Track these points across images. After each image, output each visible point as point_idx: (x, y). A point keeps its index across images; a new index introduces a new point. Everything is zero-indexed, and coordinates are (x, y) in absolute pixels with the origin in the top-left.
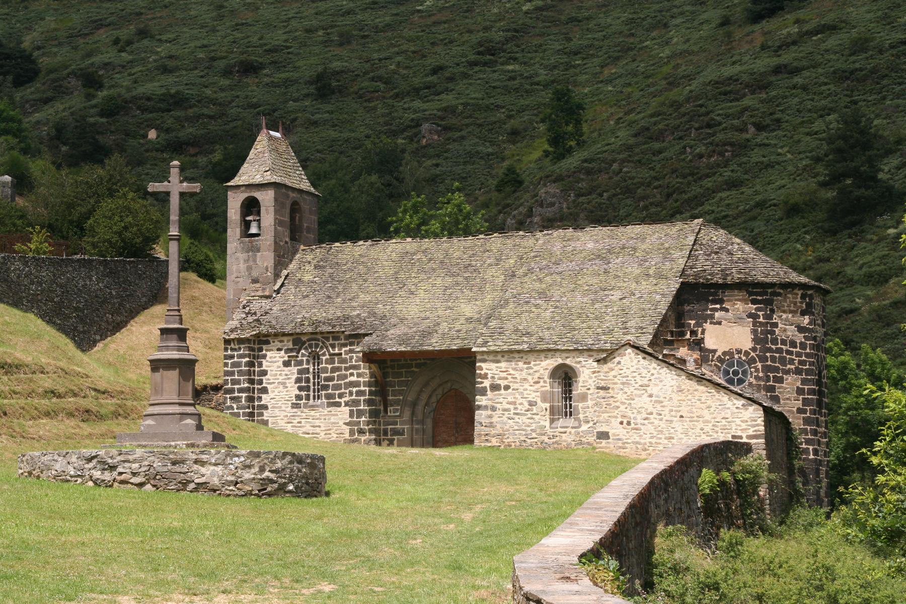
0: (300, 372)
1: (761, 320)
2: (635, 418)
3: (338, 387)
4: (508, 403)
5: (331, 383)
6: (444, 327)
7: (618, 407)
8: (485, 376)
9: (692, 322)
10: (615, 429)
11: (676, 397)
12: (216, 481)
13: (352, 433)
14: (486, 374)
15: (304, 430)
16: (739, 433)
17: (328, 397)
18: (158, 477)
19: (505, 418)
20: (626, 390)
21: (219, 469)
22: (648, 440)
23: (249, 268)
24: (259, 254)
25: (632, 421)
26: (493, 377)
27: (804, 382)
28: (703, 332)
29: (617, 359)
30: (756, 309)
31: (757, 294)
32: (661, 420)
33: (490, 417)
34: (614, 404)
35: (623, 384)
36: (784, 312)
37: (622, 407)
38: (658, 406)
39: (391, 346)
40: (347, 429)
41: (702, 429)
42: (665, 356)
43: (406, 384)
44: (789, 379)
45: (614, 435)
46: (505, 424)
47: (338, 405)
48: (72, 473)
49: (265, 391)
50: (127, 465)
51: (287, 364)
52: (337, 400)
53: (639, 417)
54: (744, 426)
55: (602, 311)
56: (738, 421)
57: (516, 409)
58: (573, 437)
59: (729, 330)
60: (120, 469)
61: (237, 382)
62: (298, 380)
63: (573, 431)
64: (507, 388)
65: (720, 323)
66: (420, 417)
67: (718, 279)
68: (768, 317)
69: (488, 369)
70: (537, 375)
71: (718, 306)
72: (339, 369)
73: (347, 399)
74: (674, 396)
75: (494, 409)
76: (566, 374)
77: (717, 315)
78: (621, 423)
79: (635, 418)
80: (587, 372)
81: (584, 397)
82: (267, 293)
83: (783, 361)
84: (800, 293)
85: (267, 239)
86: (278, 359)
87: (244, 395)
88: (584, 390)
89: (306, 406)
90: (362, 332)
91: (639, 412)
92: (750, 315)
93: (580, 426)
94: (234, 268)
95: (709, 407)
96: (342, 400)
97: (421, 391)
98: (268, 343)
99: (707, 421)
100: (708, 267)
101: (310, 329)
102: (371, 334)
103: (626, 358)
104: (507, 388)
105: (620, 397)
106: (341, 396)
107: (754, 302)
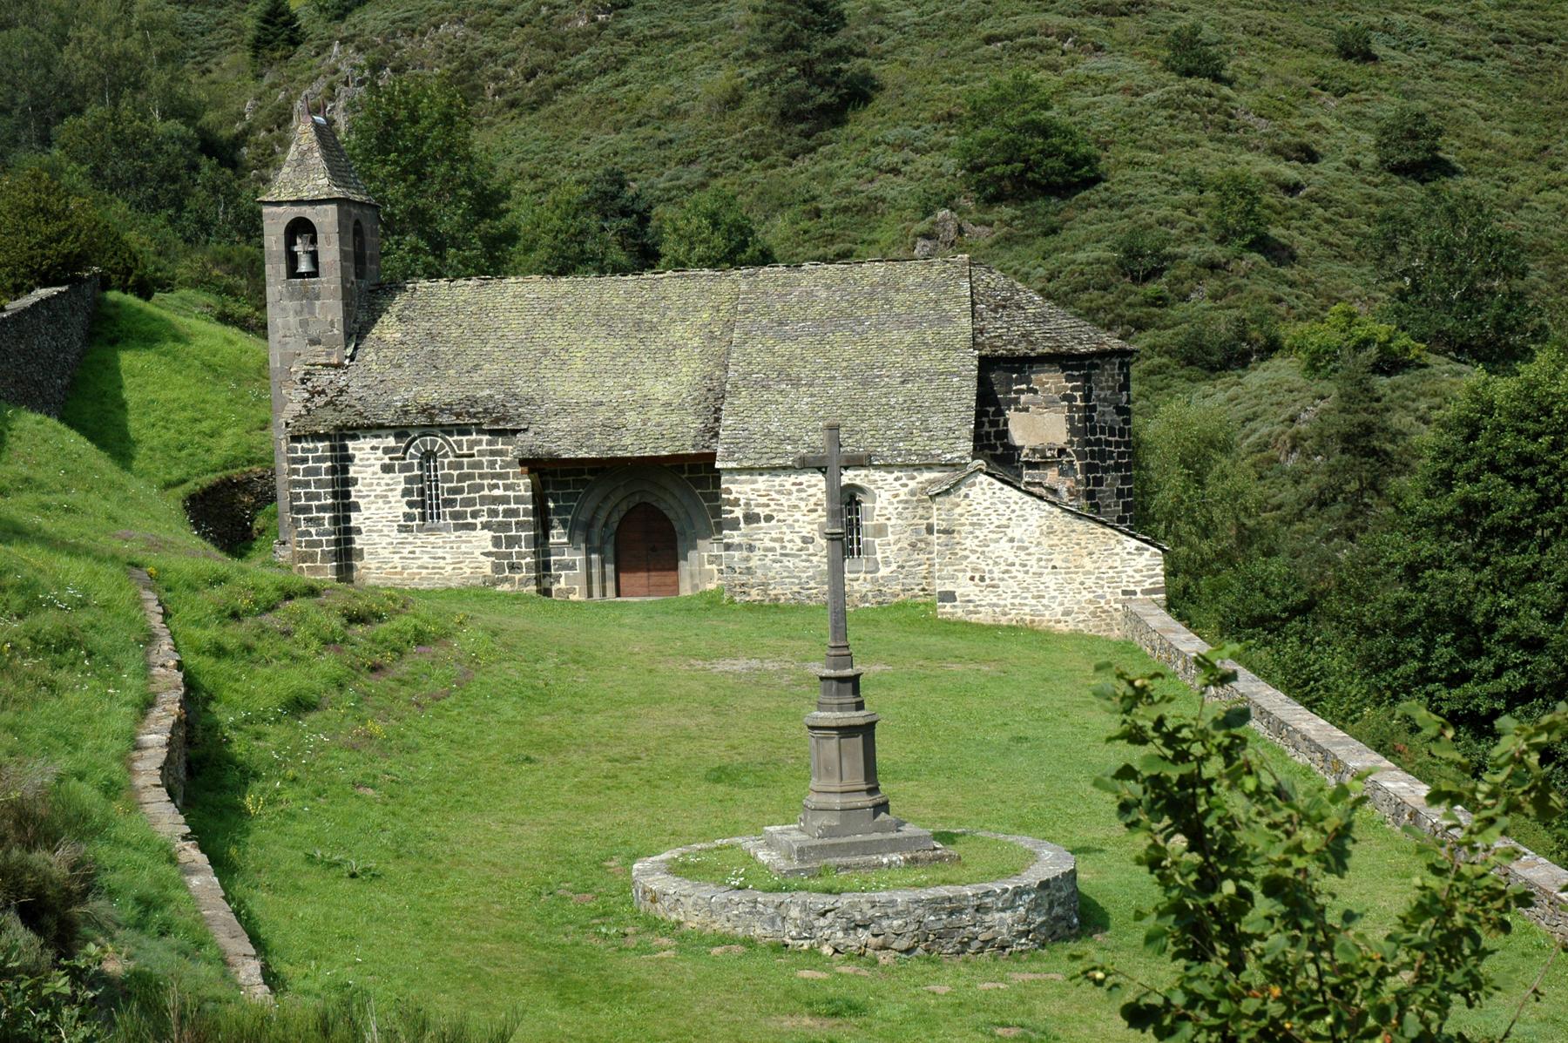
0: (408, 480)
1: (1078, 403)
2: (991, 572)
3: (469, 502)
4: (773, 540)
5: (458, 497)
6: (631, 417)
7: (966, 557)
8: (736, 503)
9: (992, 409)
10: (964, 588)
11: (1045, 541)
12: (1004, 935)
13: (497, 568)
14: (737, 500)
15: (419, 562)
16: (1132, 587)
17: (455, 516)
18: (931, 937)
19: (767, 562)
20: (977, 533)
21: (1007, 915)
22: (1009, 601)
23: (304, 324)
24: (318, 303)
25: (987, 576)
26: (747, 504)
27: (1125, 480)
28: (1006, 424)
29: (964, 490)
30: (1074, 389)
31: (1072, 368)
32: (1027, 572)
33: (747, 559)
34: (961, 553)
35: (972, 524)
36: (1102, 389)
37: (973, 558)
38: (1022, 554)
39: (567, 450)
40: (487, 566)
41: (1082, 583)
42: (1028, 483)
43: (574, 497)
44: (1109, 478)
45: (962, 595)
46: (770, 569)
47: (472, 527)
48: (794, 933)
49: (356, 507)
50: (885, 923)
51: (387, 469)
52: (470, 520)
53: (996, 569)
54: (1138, 577)
55: (884, 401)
56: (1130, 571)
57: (783, 548)
58: (869, 587)
59: (1039, 418)
60: (874, 928)
61: (317, 497)
62: (406, 492)
63: (869, 576)
64: (769, 518)
65: (1027, 410)
66: (597, 543)
67: (1022, 349)
68: (1086, 398)
69: (740, 490)
70: (813, 500)
71: (1024, 386)
72: (470, 476)
73: (485, 519)
74: (1043, 540)
75: (751, 548)
76: (853, 497)
77: (1023, 398)
78: (972, 579)
79: (991, 572)
80: (886, 495)
81: (880, 531)
82: (334, 360)
83: (1103, 456)
84: (1117, 361)
85: (331, 278)
86: (372, 461)
87: (327, 515)
88: (882, 520)
89: (420, 529)
90: (509, 426)
91: (996, 563)
92: (1065, 398)
93: (877, 570)
94: (279, 321)
95: (1091, 554)
96: (478, 521)
97: (598, 507)
98: (355, 437)
99: (1088, 573)
100: (1007, 334)
101: (423, 420)
102: (526, 430)
103: (977, 489)
104: (769, 518)
105: (969, 543)
106: (475, 515)
107: (1069, 379)
